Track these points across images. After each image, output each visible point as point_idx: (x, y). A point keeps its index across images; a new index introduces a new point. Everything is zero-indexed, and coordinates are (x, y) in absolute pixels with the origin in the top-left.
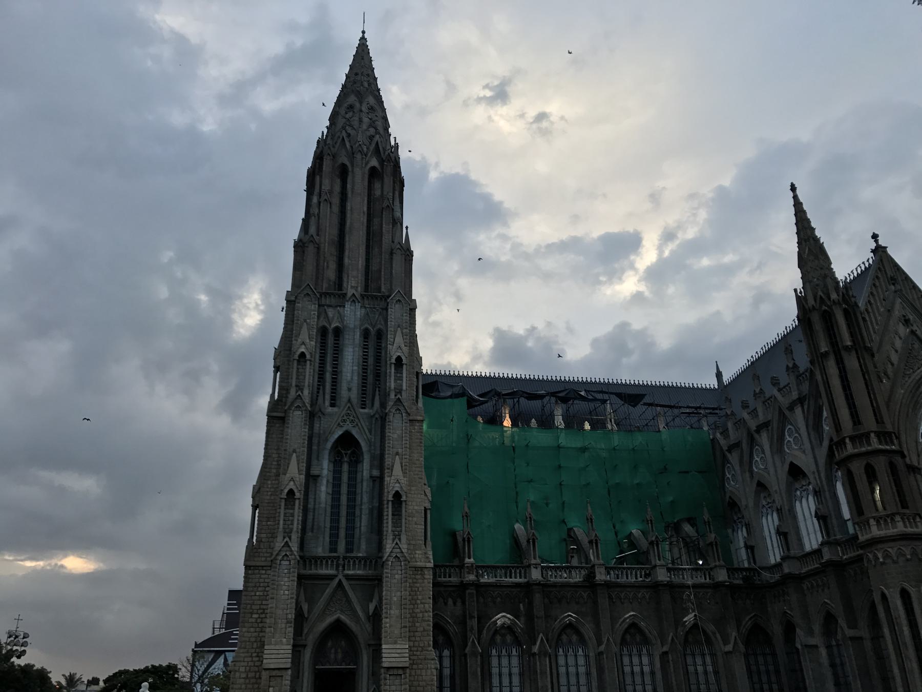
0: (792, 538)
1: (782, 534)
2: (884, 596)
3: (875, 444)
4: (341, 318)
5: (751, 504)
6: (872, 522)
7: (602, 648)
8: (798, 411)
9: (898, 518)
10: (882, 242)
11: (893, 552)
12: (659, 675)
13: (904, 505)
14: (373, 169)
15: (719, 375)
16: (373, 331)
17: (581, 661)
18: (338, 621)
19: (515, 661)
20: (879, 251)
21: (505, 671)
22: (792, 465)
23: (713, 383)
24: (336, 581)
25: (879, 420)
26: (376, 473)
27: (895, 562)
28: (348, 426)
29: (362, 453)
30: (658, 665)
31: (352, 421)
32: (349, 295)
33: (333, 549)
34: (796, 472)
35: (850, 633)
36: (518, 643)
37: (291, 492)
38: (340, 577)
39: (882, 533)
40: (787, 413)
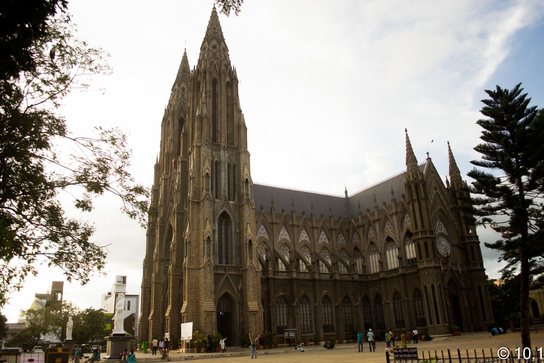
0: (384, 264)
1: (381, 262)
2: (425, 287)
3: (428, 235)
4: (219, 156)
5: (366, 249)
6: (425, 262)
7: (317, 304)
8: (395, 217)
9: (433, 261)
10: (430, 157)
11: (431, 272)
12: (334, 314)
13: (435, 257)
14: (228, 82)
15: (346, 192)
16: (232, 165)
17: (308, 309)
18: (226, 292)
19: (285, 309)
20: (429, 159)
21: (281, 313)
22: (388, 237)
23: (343, 195)
24: (225, 276)
25: (430, 227)
26: (238, 231)
27: (431, 276)
28: (225, 209)
29: (231, 221)
30: (334, 310)
31: (226, 207)
32: (222, 146)
33: (220, 262)
34: (389, 239)
35: (406, 299)
36: (286, 301)
37: (209, 237)
38: (227, 274)
39: (428, 265)
40: (389, 217)
